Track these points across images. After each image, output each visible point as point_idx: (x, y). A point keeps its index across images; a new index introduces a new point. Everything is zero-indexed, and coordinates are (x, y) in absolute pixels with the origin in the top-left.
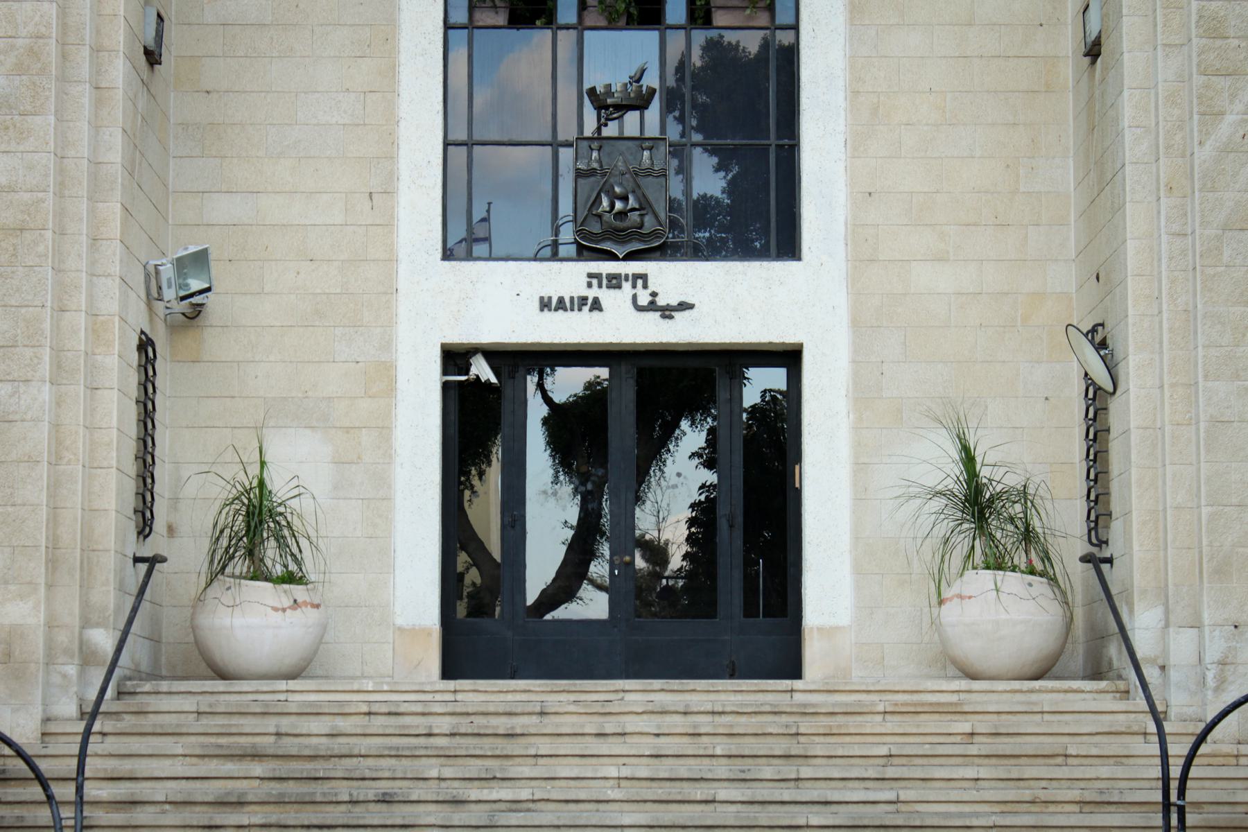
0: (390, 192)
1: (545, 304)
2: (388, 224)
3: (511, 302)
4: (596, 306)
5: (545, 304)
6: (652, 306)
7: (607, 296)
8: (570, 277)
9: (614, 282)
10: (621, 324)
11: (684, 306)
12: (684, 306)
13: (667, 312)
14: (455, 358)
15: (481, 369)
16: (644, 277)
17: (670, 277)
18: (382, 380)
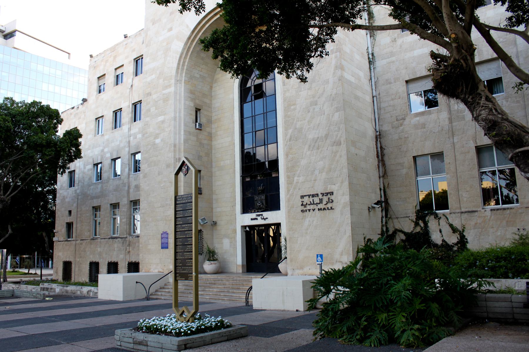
1: (252, 219)
2: (234, 210)
3: (248, 219)
4: (257, 219)
5: (252, 219)
6: (263, 219)
7: (258, 218)
8: (254, 215)
9: (259, 215)
10: (260, 222)
11: (267, 218)
12: (267, 218)
13: (265, 219)
14: (244, 227)
15: (248, 229)
16: (262, 215)
17: (265, 214)
18: (235, 231)
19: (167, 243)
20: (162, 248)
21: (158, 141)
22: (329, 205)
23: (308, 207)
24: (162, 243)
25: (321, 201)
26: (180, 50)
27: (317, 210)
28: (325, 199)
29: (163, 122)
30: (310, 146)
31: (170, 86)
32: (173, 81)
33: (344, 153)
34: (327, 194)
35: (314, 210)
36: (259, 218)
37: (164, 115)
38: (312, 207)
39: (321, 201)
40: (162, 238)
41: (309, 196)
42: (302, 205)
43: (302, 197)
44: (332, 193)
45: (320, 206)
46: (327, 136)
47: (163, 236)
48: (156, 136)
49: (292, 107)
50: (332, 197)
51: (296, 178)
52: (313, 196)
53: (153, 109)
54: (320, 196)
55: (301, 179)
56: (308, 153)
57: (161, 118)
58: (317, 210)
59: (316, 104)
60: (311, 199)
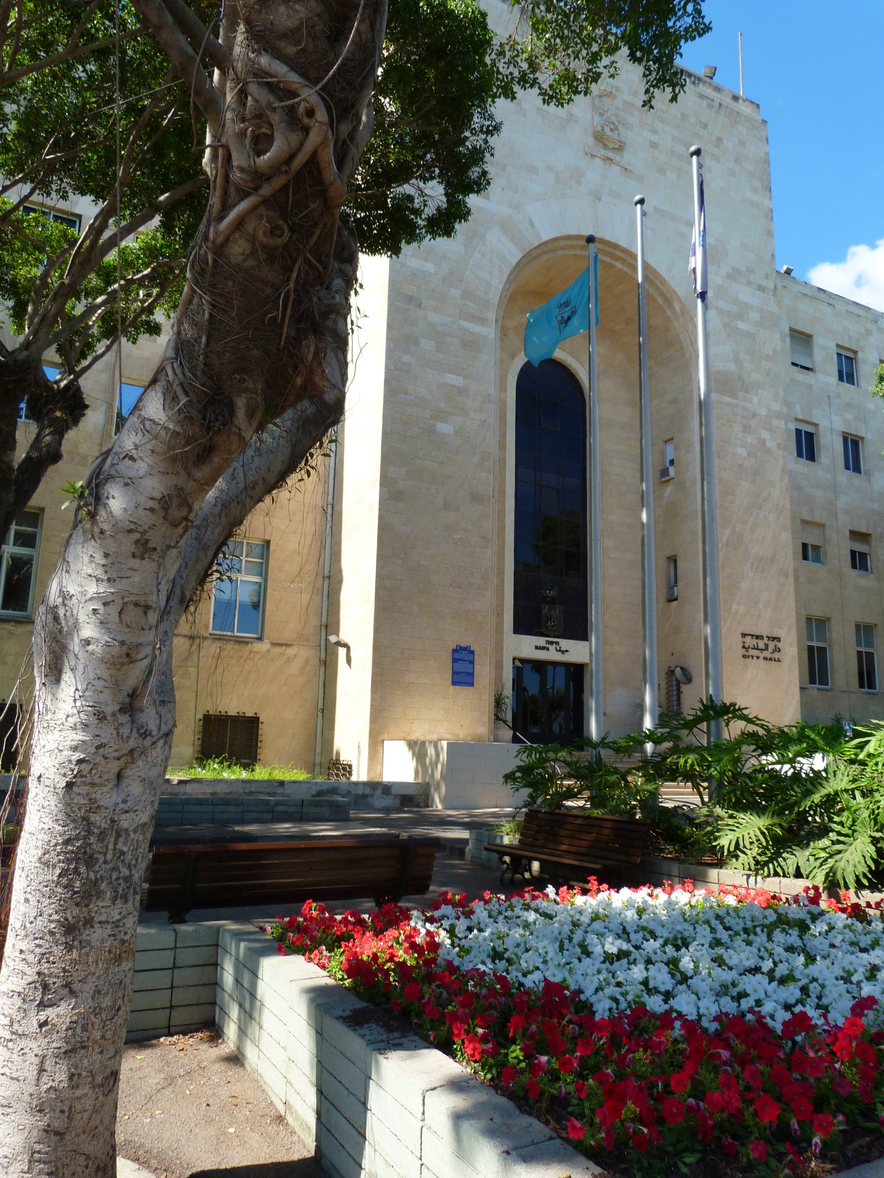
0: (503, 614)
1: (537, 648)
5: (537, 648)
7: (550, 647)
8: (541, 641)
9: (551, 643)
10: (552, 655)
13: (563, 652)
17: (564, 643)
19: (472, 674)
20: (454, 683)
21: (444, 428)
22: (776, 655)
23: (752, 652)
24: (454, 673)
25: (767, 645)
26: (514, 261)
27: (761, 659)
28: (771, 645)
29: (462, 391)
30: (752, 564)
31: (482, 321)
32: (492, 315)
33: (791, 589)
34: (774, 639)
35: (758, 658)
36: (552, 648)
37: (466, 377)
38: (755, 653)
39: (767, 645)
40: (455, 660)
41: (753, 636)
42: (744, 647)
43: (744, 635)
44: (779, 639)
45: (766, 654)
46: (773, 559)
47: (457, 656)
48: (440, 415)
49: (730, 497)
50: (779, 645)
51: (734, 606)
52: (758, 637)
53: (427, 345)
54: (766, 639)
55: (742, 609)
56: (751, 574)
57: (452, 379)
58: (761, 659)
59: (760, 509)
60: (755, 641)
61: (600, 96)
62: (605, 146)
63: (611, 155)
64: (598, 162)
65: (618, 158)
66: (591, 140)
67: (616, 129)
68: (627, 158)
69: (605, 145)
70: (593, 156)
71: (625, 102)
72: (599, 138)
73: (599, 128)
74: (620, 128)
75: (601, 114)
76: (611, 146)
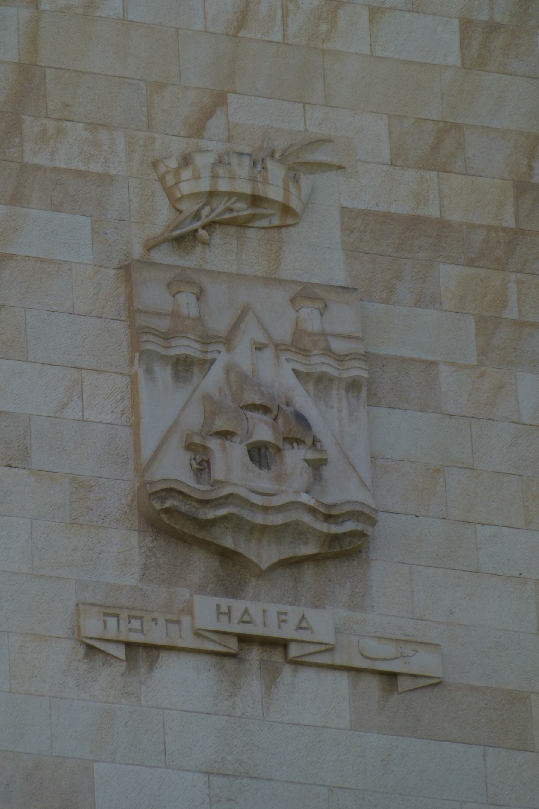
61: (183, 241)
62: (232, 570)
63: (263, 612)
64: (182, 682)
65: (322, 624)
66: (120, 554)
67: (299, 430)
68: (388, 608)
69: (226, 555)
70: (141, 653)
71: (363, 227)
72: (181, 524)
73: (175, 467)
74: (327, 418)
75: (183, 367)
76: (266, 554)
